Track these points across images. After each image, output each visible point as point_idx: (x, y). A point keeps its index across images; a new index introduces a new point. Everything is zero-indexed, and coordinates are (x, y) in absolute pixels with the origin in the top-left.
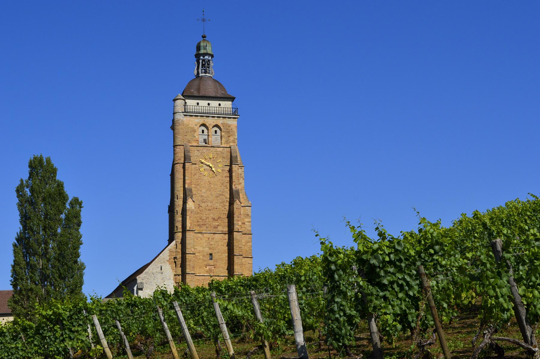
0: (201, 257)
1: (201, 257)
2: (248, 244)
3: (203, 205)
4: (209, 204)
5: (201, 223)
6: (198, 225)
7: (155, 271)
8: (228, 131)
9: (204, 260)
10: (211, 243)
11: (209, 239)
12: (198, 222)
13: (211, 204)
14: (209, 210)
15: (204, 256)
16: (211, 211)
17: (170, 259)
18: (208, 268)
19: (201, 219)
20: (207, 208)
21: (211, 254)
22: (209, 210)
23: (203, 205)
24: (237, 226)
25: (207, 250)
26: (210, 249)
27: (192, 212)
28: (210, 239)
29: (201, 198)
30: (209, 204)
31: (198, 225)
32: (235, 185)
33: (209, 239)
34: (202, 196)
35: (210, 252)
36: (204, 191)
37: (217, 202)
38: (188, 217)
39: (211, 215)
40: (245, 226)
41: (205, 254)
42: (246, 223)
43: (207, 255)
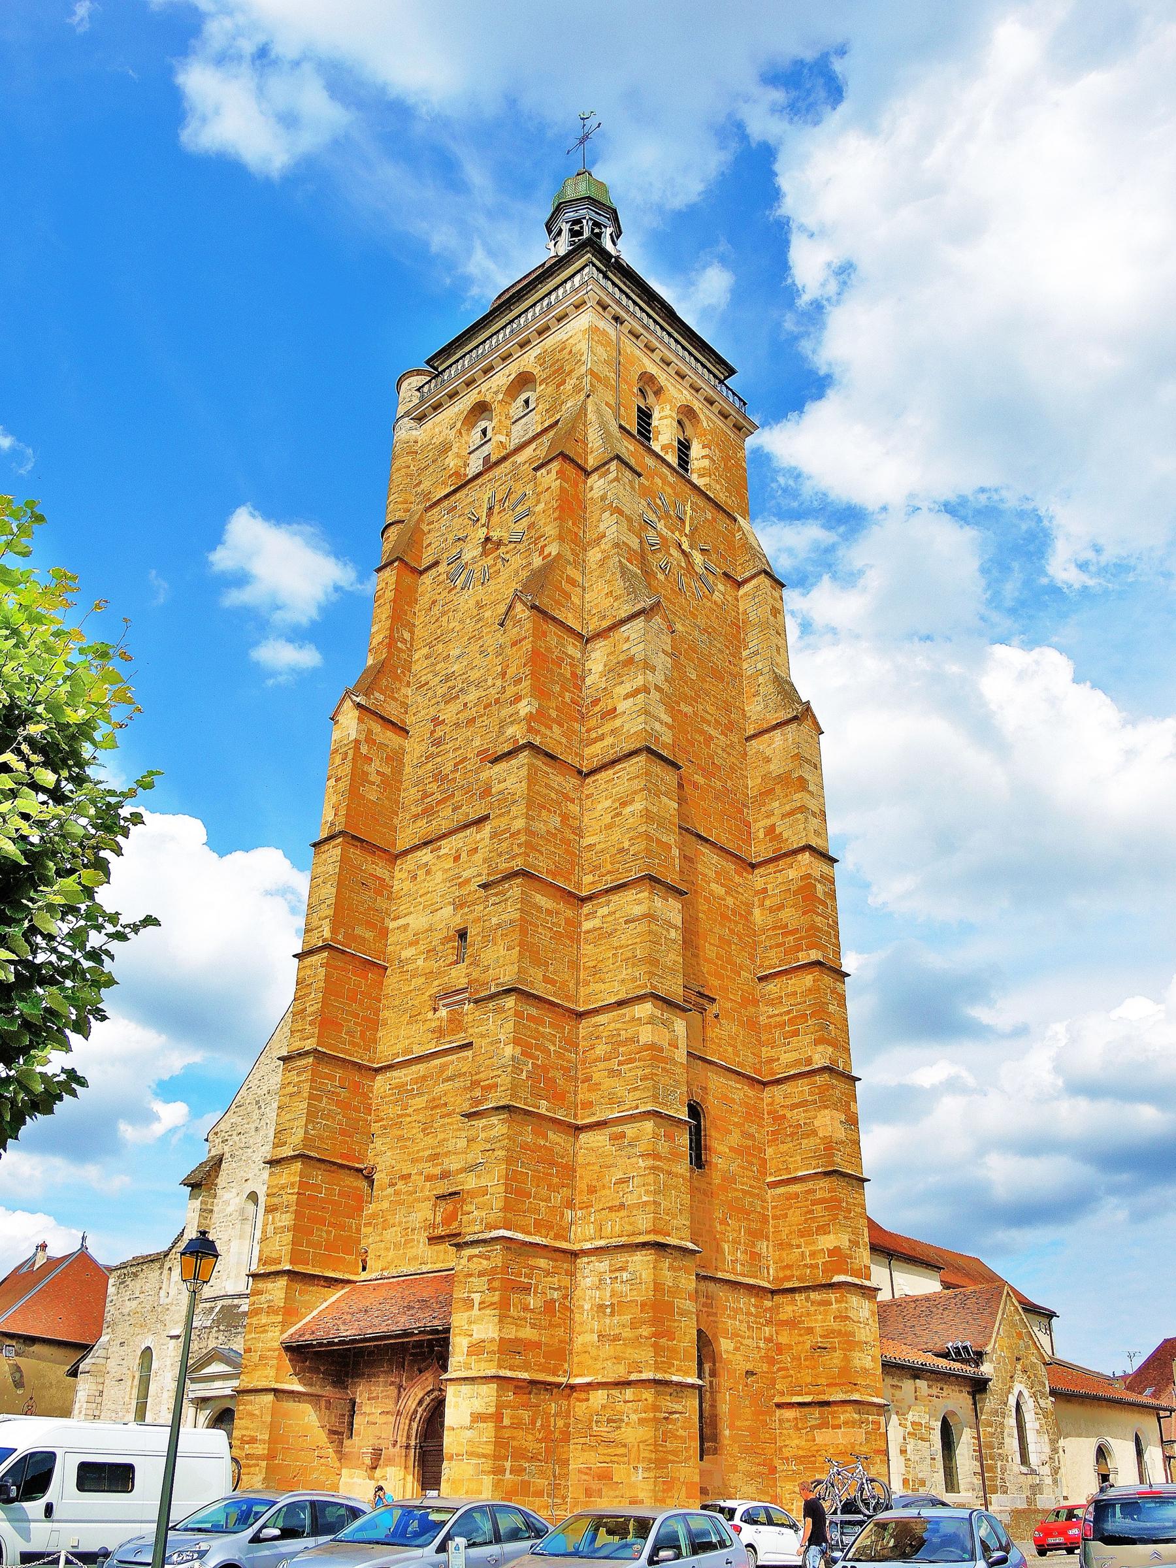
0: (420, 962)
2: (627, 810)
10: (465, 875)
11: (457, 859)
12: (426, 795)
15: (431, 952)
18: (443, 1012)
21: (462, 935)
23: (449, 713)
25: (448, 918)
26: (459, 905)
28: (464, 855)
33: (457, 859)
35: (457, 922)
36: (457, 652)
40: (618, 723)
42: (622, 706)
43: (446, 940)
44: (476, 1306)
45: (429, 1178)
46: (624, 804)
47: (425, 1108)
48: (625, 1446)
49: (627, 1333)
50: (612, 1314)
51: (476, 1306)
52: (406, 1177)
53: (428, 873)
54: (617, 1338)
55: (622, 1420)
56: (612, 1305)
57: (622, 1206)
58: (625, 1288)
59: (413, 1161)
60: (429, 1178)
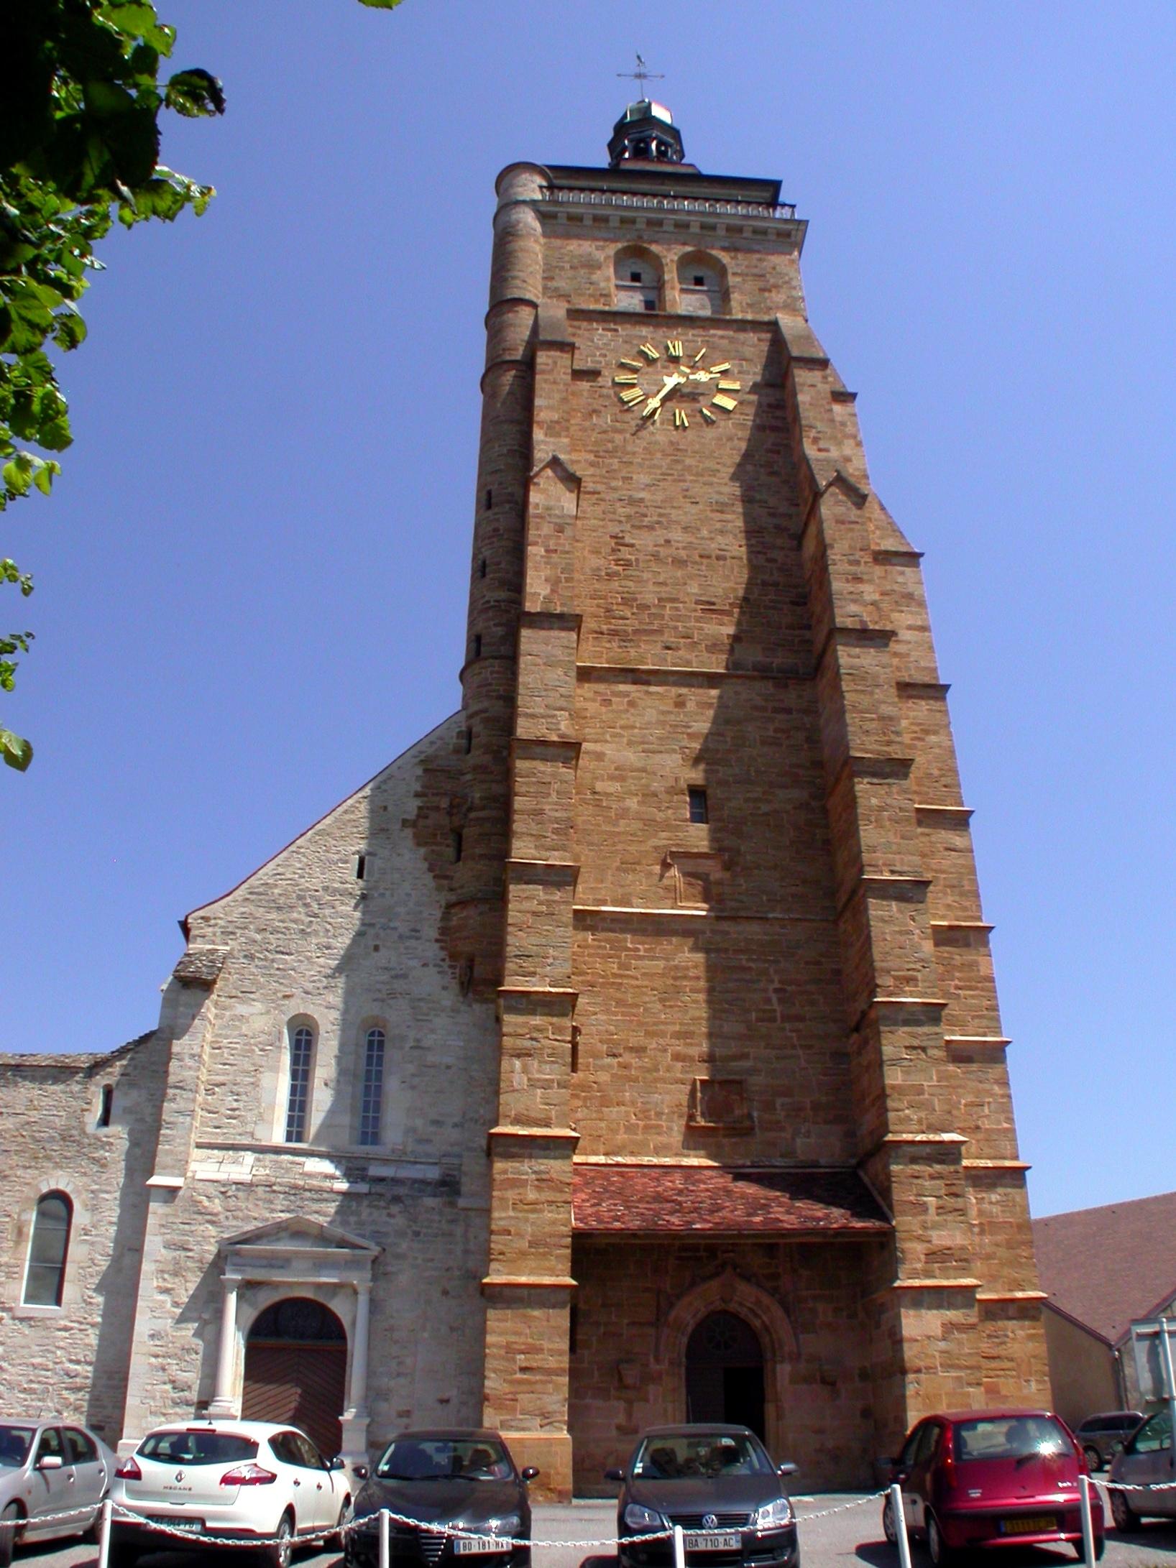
0: (632, 803)
1: (632, 803)
3: (645, 541)
4: (677, 535)
5: (631, 625)
6: (614, 633)
7: (316, 883)
8: (755, 271)
9: (649, 822)
13: (687, 538)
14: (679, 563)
15: (648, 796)
16: (690, 569)
17: (422, 813)
19: (626, 602)
20: (663, 552)
22: (679, 563)
24: (853, 608)
27: (560, 529)
29: (630, 510)
30: (677, 535)
31: (614, 633)
32: (816, 440)
34: (632, 502)
37: (722, 532)
38: (535, 552)
39: (694, 588)
41: (655, 786)
43: (672, 791)
44: (932, 1210)
45: (677, 1057)
46: (927, 732)
47: (663, 975)
48: (1012, 1360)
49: (1002, 1252)
50: (982, 1232)
51: (932, 1210)
52: (639, 1050)
53: (632, 704)
54: (989, 1257)
55: (1007, 1336)
56: (981, 1224)
57: (978, 1128)
58: (995, 1209)
59: (649, 1034)
60: (677, 1057)
